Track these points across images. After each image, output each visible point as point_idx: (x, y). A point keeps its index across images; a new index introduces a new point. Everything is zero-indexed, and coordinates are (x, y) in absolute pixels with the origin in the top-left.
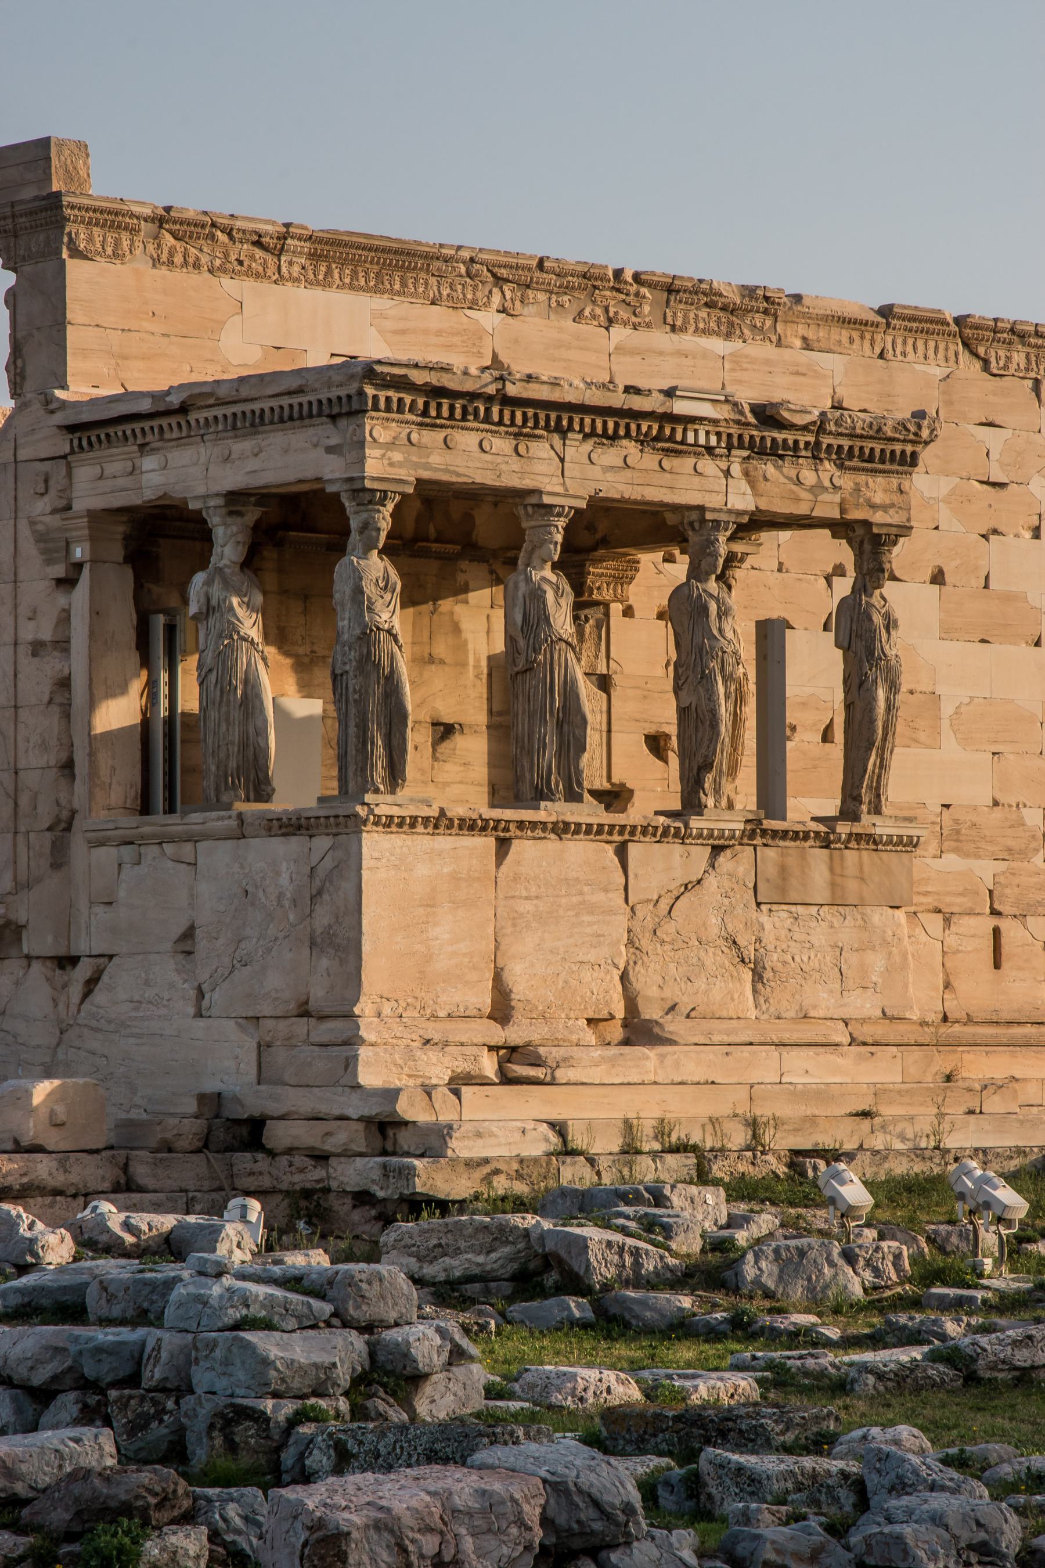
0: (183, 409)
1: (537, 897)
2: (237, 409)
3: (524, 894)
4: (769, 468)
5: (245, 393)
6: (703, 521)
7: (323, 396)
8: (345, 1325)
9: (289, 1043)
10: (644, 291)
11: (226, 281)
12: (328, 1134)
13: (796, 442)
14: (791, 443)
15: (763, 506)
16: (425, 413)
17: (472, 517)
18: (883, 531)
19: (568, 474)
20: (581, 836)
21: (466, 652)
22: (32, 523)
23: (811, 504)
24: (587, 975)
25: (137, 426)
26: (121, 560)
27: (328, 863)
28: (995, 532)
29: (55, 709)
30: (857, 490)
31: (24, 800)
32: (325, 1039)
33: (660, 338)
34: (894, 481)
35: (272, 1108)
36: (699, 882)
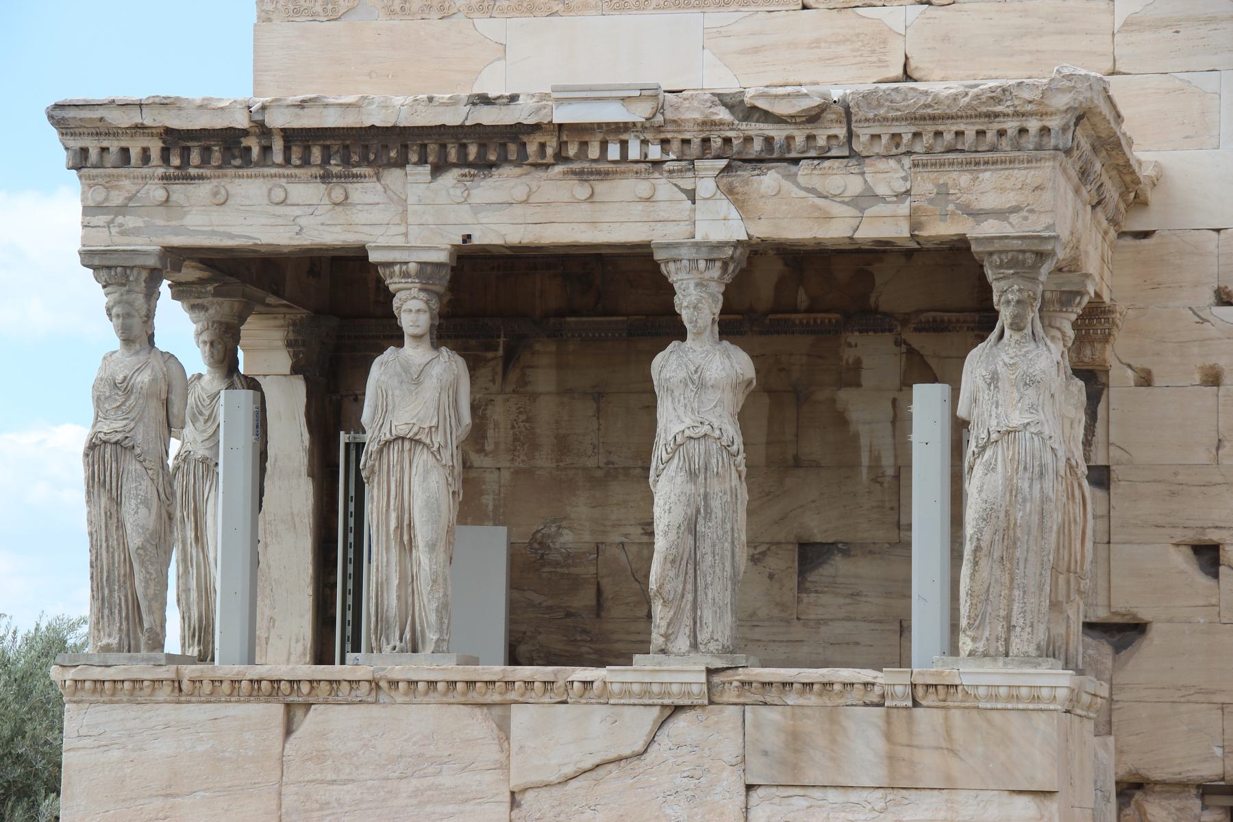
1: (353, 781)
3: (331, 776)
4: (770, 180)
6: (667, 262)
13: (811, 138)
14: (800, 139)
15: (763, 230)
16: (166, 160)
17: (870, 277)
18: (997, 246)
21: (857, 449)
23: (855, 222)
26: (288, 372)
30: (943, 192)
34: (1020, 175)
36: (639, 755)
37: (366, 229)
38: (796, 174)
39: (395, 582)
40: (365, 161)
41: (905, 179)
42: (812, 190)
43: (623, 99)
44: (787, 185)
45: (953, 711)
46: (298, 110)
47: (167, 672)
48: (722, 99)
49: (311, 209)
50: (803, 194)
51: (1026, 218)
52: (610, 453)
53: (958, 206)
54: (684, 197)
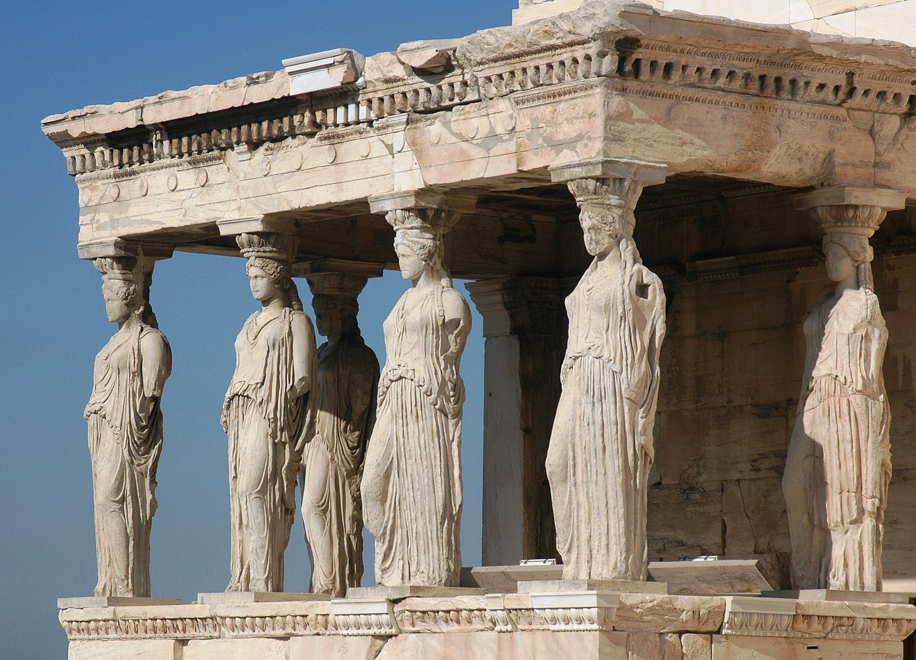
4: (434, 128)
15: (434, 179)
18: (565, 176)
20: (248, 632)
37: (219, 206)
38: (449, 122)
39: (237, 526)
41: (511, 117)
42: (459, 135)
43: (328, 66)
44: (445, 131)
45: (538, 633)
46: (157, 106)
47: (108, 613)
49: (189, 193)
50: (454, 139)
51: (586, 146)
52: (730, 391)
53: (545, 140)
54: (386, 151)
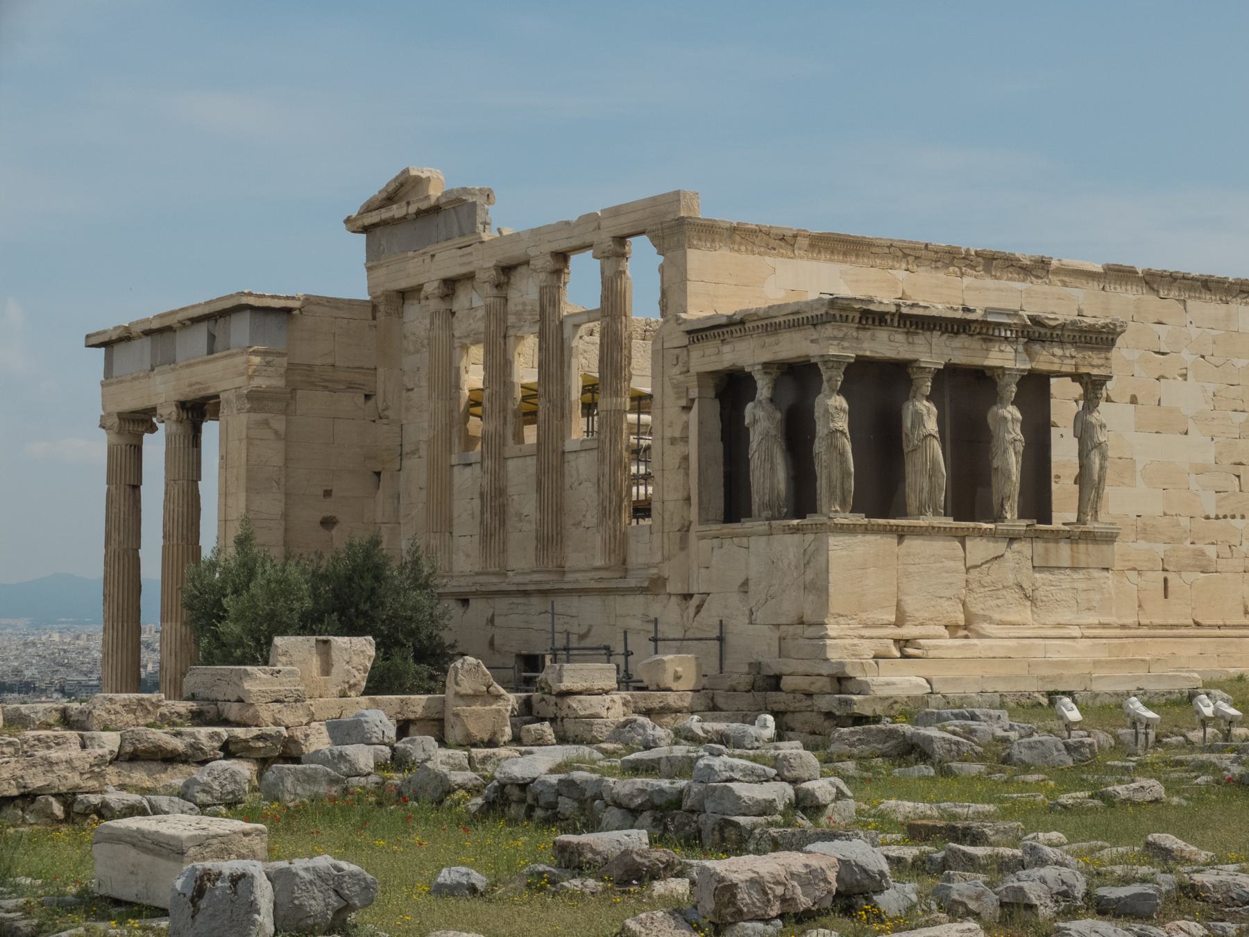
0: (742, 322)
2: (767, 321)
4: (1037, 347)
5: (771, 314)
7: (809, 315)
8: (783, 780)
9: (794, 637)
10: (980, 259)
11: (766, 258)
12: (813, 683)
16: (860, 322)
19: (932, 353)
22: (671, 379)
24: (946, 604)
25: (720, 331)
27: (812, 548)
28: (1163, 377)
29: (682, 471)
31: (667, 516)
32: (811, 635)
33: (989, 282)
35: (786, 670)
40: (922, 328)
48: (1031, 318)
